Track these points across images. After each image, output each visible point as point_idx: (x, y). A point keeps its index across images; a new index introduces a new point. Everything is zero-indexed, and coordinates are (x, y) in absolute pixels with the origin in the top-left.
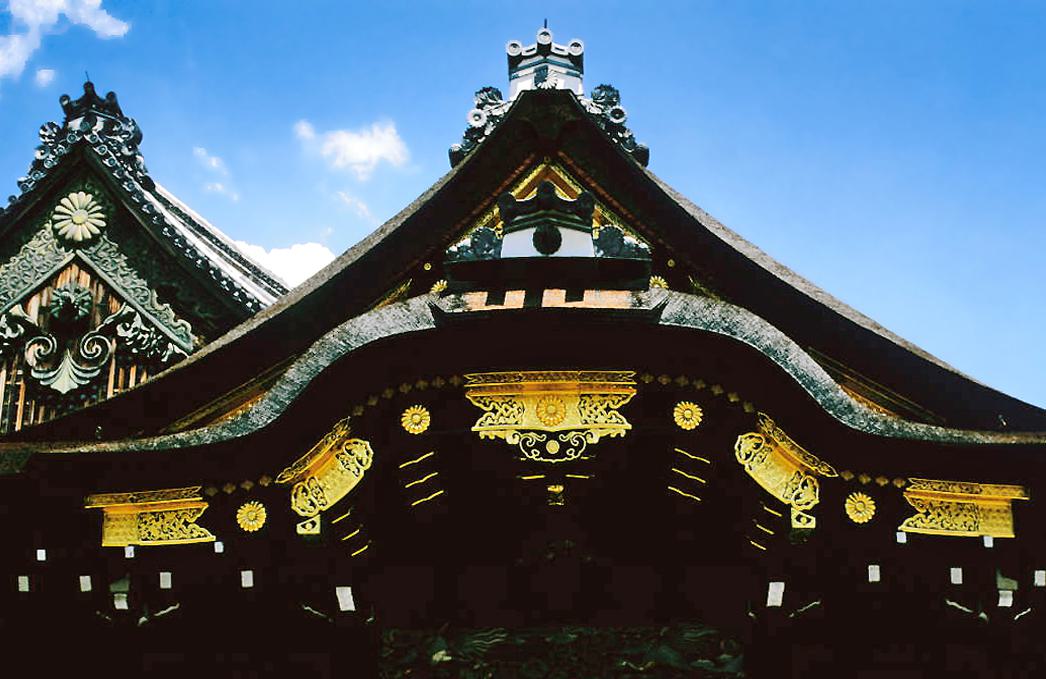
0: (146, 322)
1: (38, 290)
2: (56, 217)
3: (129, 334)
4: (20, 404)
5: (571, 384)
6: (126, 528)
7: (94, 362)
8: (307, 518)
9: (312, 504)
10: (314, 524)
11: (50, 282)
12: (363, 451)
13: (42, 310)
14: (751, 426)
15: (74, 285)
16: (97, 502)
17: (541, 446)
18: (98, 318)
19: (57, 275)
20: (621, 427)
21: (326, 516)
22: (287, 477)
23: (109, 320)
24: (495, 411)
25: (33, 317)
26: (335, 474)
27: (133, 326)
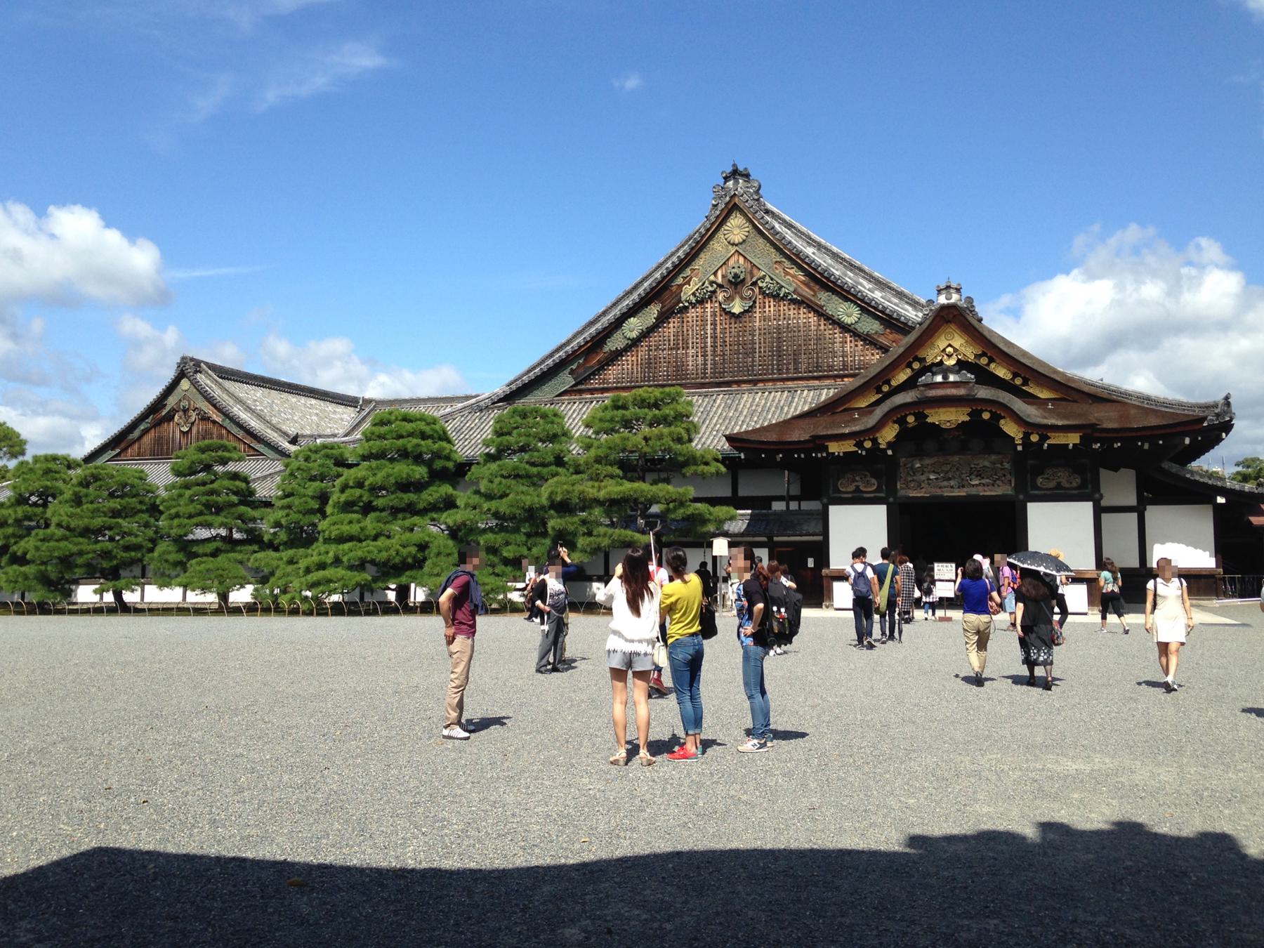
5: (953, 410)
6: (835, 448)
12: (896, 426)
13: (723, 276)
15: (737, 264)
20: (968, 419)
25: (720, 280)
26: (889, 434)
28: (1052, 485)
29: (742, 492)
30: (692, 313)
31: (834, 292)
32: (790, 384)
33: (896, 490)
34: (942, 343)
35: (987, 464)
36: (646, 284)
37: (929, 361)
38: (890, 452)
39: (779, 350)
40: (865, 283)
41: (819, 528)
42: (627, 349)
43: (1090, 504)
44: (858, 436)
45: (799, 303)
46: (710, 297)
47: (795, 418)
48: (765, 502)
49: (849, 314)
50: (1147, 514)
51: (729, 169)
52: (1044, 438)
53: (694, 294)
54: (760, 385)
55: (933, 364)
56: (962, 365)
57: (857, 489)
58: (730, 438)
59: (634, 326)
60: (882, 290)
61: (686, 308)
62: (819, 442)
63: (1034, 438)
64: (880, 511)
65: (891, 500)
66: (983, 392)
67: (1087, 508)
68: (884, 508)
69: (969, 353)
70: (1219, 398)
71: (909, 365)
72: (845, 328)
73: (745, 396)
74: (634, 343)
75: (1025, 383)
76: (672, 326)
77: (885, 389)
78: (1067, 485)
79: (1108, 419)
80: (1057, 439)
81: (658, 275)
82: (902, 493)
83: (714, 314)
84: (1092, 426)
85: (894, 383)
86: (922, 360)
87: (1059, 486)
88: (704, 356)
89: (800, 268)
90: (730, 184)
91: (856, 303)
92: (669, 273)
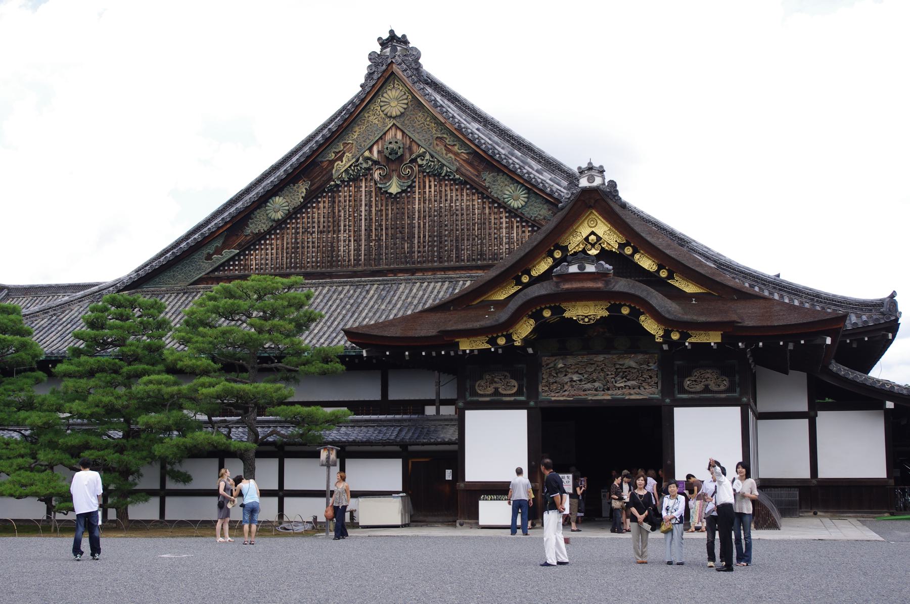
0: (432, 156)
1: (377, 141)
2: (382, 104)
3: (424, 162)
6: (466, 346)
7: (409, 177)
11: (381, 138)
12: (532, 322)
13: (379, 152)
14: (643, 313)
17: (583, 319)
18: (408, 155)
19: (385, 134)
22: (511, 331)
23: (413, 157)
26: (524, 329)
28: (699, 387)
29: (393, 396)
30: (344, 193)
31: (499, 171)
32: (452, 274)
33: (537, 393)
34: (584, 231)
35: (633, 364)
36: (294, 159)
38: (530, 351)
39: (440, 236)
40: (533, 163)
41: (455, 437)
42: (269, 232)
43: (739, 408)
44: (491, 332)
45: (464, 183)
47: (421, 312)
48: (418, 406)
49: (517, 199)
50: (817, 418)
51: (385, 36)
52: (685, 336)
53: (346, 171)
54: (419, 275)
55: (576, 253)
56: (605, 255)
57: (496, 392)
58: (350, 334)
59: (279, 206)
60: (553, 172)
61: (337, 186)
62: (448, 339)
64: (520, 418)
65: (532, 403)
66: (622, 285)
67: (737, 411)
68: (523, 414)
69: (611, 239)
70: (883, 294)
71: (550, 254)
72: (513, 213)
73: (402, 286)
74: (280, 225)
75: (670, 276)
76: (322, 208)
77: (525, 279)
78: (716, 389)
79: (748, 316)
80: (698, 338)
81: (306, 149)
82: (543, 396)
84: (731, 323)
85: (535, 273)
86: (564, 249)
87: (707, 389)
88: (357, 241)
89: (463, 144)
90: (388, 51)
91: (523, 185)
92: (320, 146)
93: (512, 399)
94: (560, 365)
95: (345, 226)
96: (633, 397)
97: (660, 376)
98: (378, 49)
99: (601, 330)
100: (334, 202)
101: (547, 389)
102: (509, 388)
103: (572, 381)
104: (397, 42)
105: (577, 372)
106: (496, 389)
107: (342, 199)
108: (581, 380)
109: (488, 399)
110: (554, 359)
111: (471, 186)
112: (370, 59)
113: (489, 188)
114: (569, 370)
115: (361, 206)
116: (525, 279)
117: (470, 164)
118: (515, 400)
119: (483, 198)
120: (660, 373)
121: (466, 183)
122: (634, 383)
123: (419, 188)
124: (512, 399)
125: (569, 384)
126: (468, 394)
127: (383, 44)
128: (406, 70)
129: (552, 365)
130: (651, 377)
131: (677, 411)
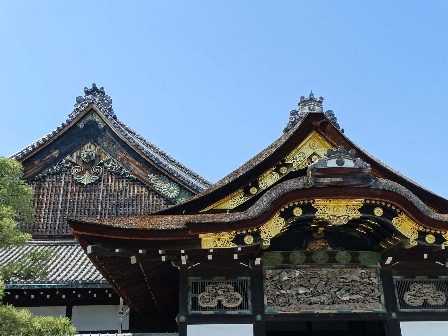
4: (70, 188)
7: (97, 175)
8: (266, 240)
9: (267, 236)
10: (268, 242)
12: (282, 220)
14: (396, 215)
16: (200, 236)
18: (97, 161)
21: (271, 240)
23: (101, 161)
24: (321, 210)
26: (274, 227)
27: (110, 163)
28: (420, 302)
30: (48, 182)
31: (161, 173)
37: (295, 168)
46: (65, 172)
51: (90, 87)
57: (220, 306)
63: (430, 239)
77: (253, 191)
78: (434, 303)
82: (269, 310)
83: (67, 184)
87: (426, 304)
88: (55, 214)
90: (90, 97)
91: (177, 183)
93: (237, 312)
94: (286, 278)
95: (46, 204)
96: (358, 311)
97: (382, 290)
98: (83, 95)
99: (323, 244)
100: (40, 187)
101: (271, 301)
102: (233, 300)
103: (298, 294)
104: (96, 92)
105: (302, 286)
106: (220, 302)
107: (46, 186)
108: (305, 294)
109: (211, 312)
110: (278, 271)
111: (141, 183)
112: (77, 101)
113: (153, 184)
114: (294, 283)
115: (60, 190)
116: (253, 191)
117: (140, 168)
118: (240, 313)
119: (149, 191)
120: (381, 287)
121: (137, 180)
122: (358, 296)
123: (104, 181)
124: (237, 312)
125: (295, 297)
126: (189, 307)
127: (87, 93)
128: (101, 108)
129: (277, 278)
130: (373, 291)
131: (402, 324)
